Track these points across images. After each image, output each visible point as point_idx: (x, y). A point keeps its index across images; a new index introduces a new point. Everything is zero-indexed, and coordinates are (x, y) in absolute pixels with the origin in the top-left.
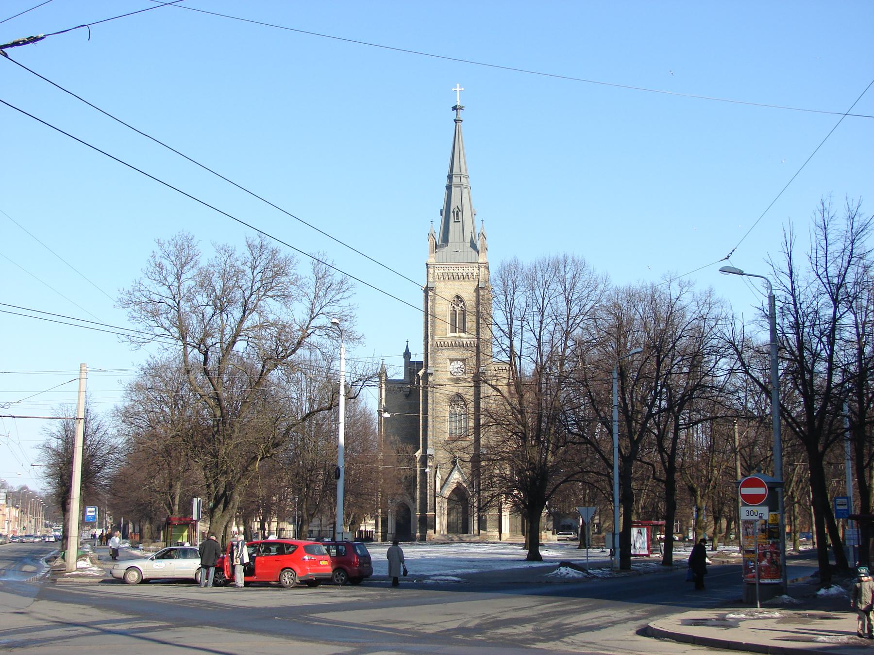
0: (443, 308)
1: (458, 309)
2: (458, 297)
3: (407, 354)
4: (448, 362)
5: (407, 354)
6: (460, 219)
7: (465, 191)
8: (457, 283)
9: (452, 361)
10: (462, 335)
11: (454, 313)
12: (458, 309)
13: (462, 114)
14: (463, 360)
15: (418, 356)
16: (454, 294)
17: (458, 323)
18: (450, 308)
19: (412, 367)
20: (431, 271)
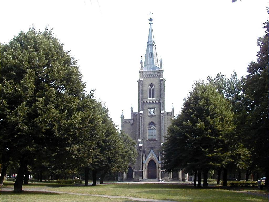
0: (146, 88)
1: (152, 89)
2: (151, 84)
3: (132, 109)
4: (148, 110)
5: (132, 109)
6: (152, 56)
7: (154, 47)
8: (151, 79)
9: (149, 109)
10: (154, 98)
11: (150, 90)
12: (152, 89)
13: (152, 22)
14: (154, 109)
15: (136, 110)
16: (150, 82)
17: (152, 93)
19: (133, 115)
20: (141, 74)
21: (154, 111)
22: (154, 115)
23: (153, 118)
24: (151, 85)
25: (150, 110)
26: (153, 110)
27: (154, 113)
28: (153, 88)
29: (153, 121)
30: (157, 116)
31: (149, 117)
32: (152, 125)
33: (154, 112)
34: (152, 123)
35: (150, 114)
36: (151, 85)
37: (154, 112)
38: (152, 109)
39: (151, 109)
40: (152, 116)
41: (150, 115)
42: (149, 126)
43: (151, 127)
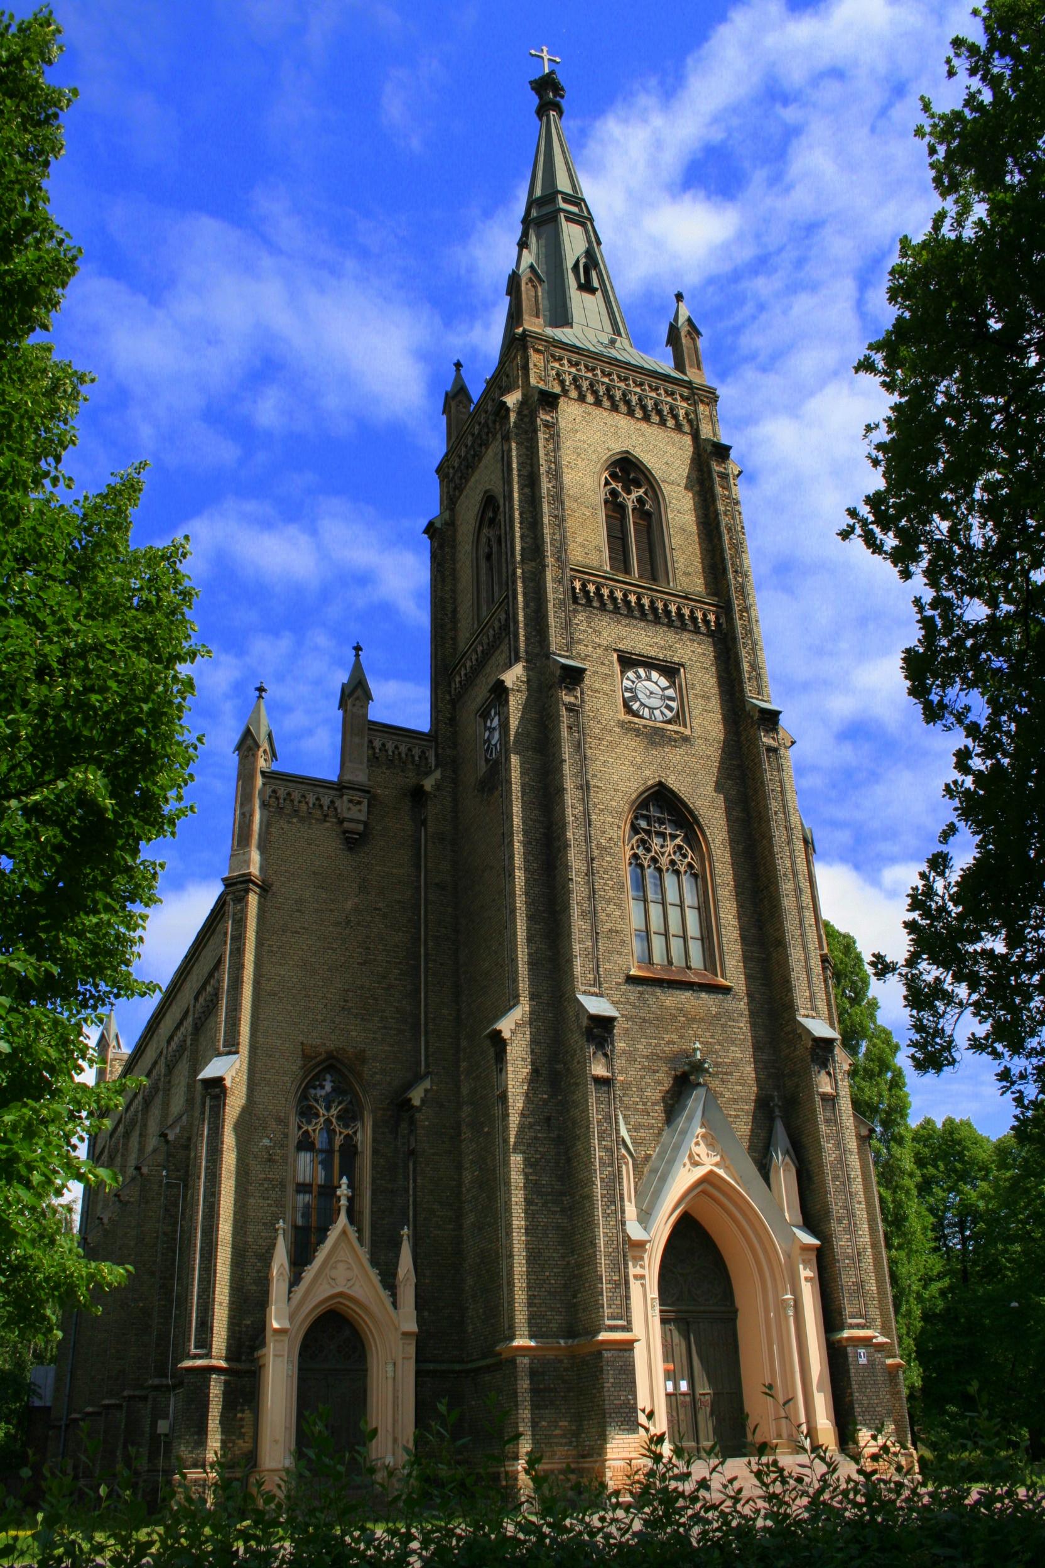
1: (630, 500)
4: (617, 667)
9: (628, 661)
12: (630, 500)
14: (670, 671)
18: (602, 493)
21: (670, 692)
22: (670, 727)
23: (676, 756)
24: (626, 469)
25: (631, 674)
26: (663, 682)
27: (669, 715)
28: (640, 500)
29: (672, 782)
30: (700, 747)
31: (630, 742)
32: (661, 822)
33: (674, 704)
34: (661, 806)
35: (636, 714)
36: (626, 469)
37: (674, 704)
38: (655, 675)
39: (641, 671)
40: (655, 737)
41: (636, 720)
42: (635, 829)
43: (656, 842)
